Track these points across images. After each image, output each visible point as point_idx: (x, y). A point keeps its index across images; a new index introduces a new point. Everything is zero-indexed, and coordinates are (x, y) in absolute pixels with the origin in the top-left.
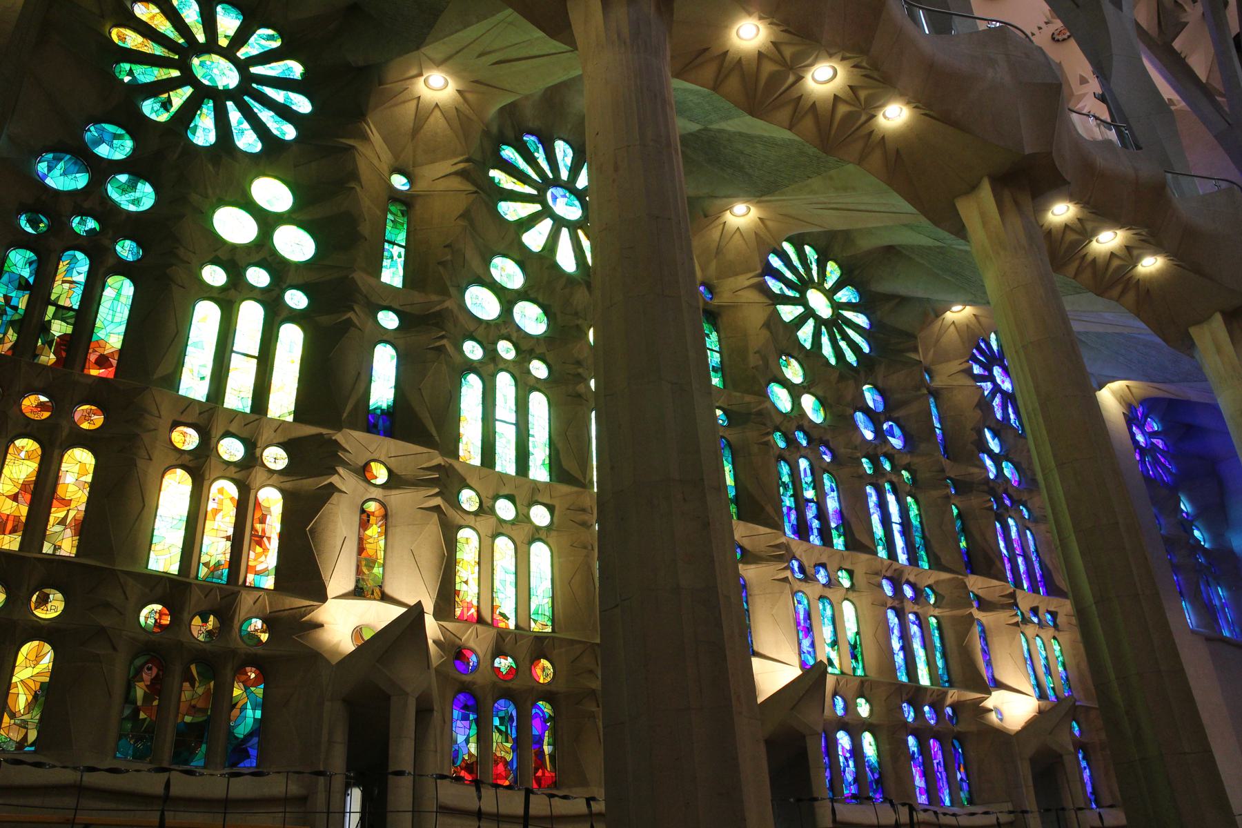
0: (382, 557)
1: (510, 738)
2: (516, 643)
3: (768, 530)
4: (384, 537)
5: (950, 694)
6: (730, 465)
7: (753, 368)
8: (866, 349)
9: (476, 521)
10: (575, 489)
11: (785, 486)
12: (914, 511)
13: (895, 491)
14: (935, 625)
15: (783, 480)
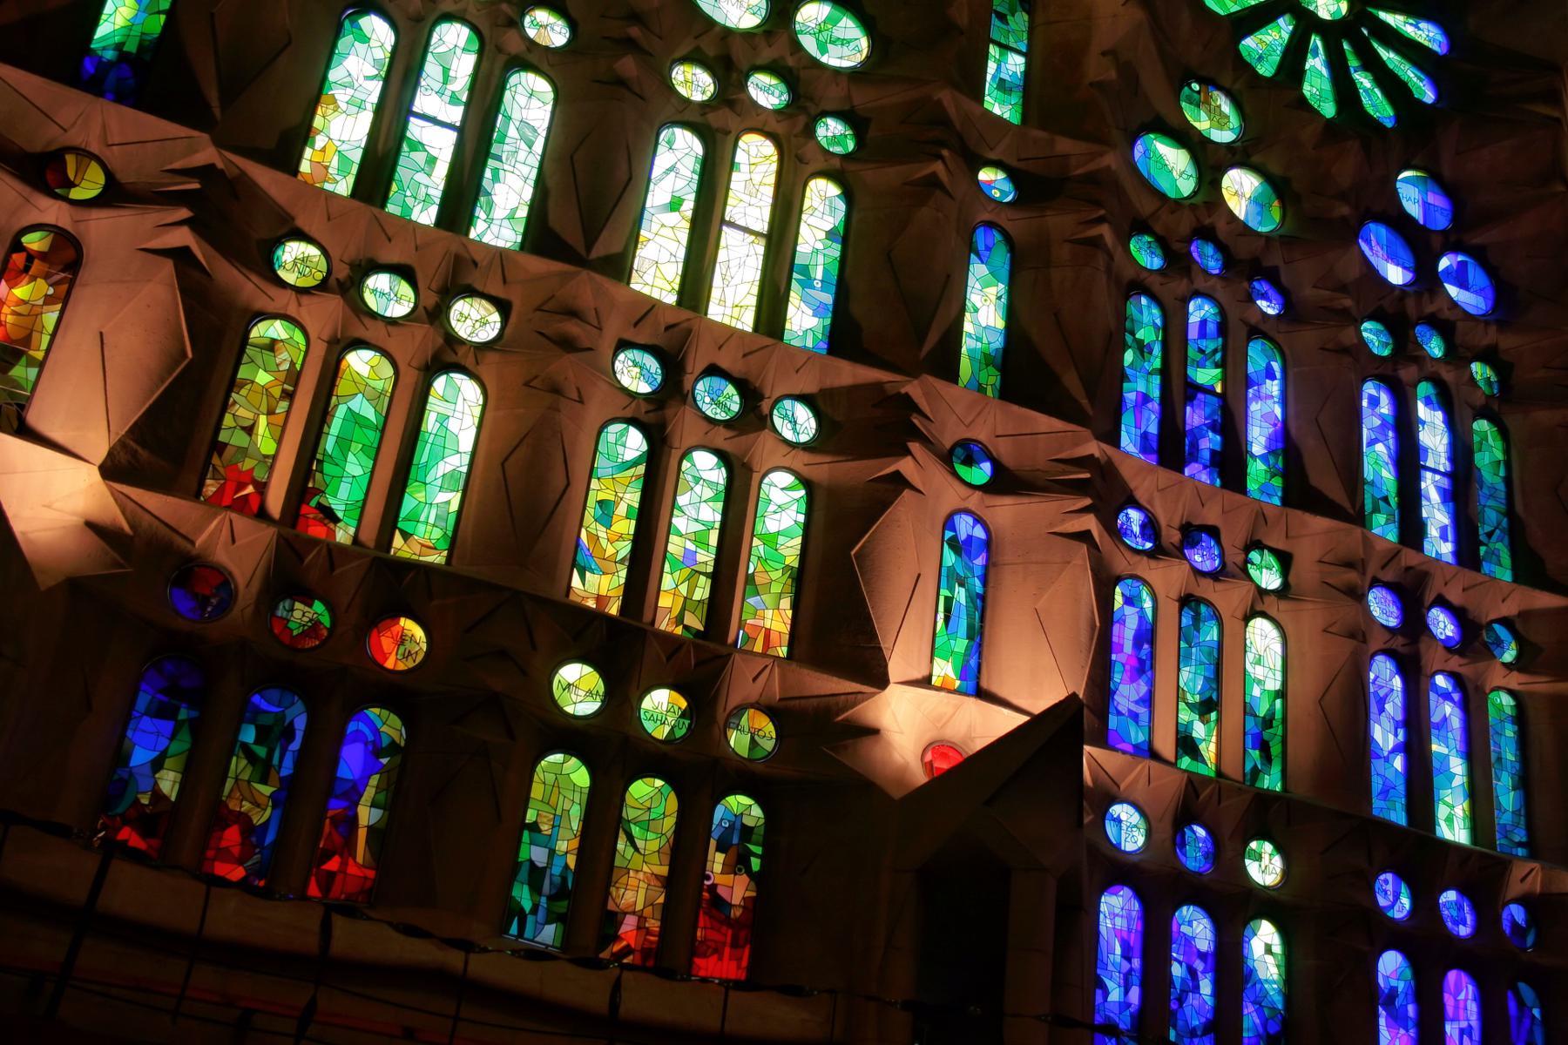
0: (44, 346)
1: (273, 773)
2: (332, 567)
3: (1057, 424)
4: (59, 306)
5: (1519, 870)
6: (1001, 286)
7: (1091, 84)
8: (1425, 92)
9: (300, 305)
10: (557, 266)
11: (1143, 349)
12: (1489, 452)
13: (1445, 401)
14: (1509, 711)
15: (1138, 336)
